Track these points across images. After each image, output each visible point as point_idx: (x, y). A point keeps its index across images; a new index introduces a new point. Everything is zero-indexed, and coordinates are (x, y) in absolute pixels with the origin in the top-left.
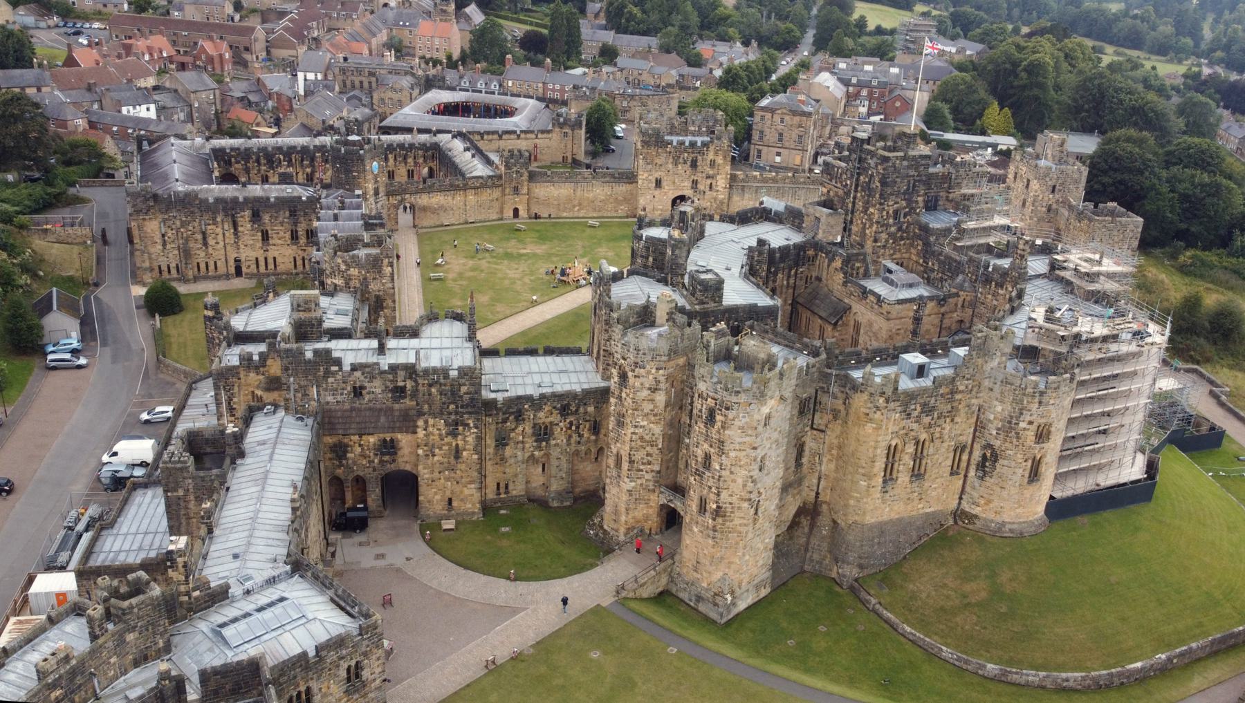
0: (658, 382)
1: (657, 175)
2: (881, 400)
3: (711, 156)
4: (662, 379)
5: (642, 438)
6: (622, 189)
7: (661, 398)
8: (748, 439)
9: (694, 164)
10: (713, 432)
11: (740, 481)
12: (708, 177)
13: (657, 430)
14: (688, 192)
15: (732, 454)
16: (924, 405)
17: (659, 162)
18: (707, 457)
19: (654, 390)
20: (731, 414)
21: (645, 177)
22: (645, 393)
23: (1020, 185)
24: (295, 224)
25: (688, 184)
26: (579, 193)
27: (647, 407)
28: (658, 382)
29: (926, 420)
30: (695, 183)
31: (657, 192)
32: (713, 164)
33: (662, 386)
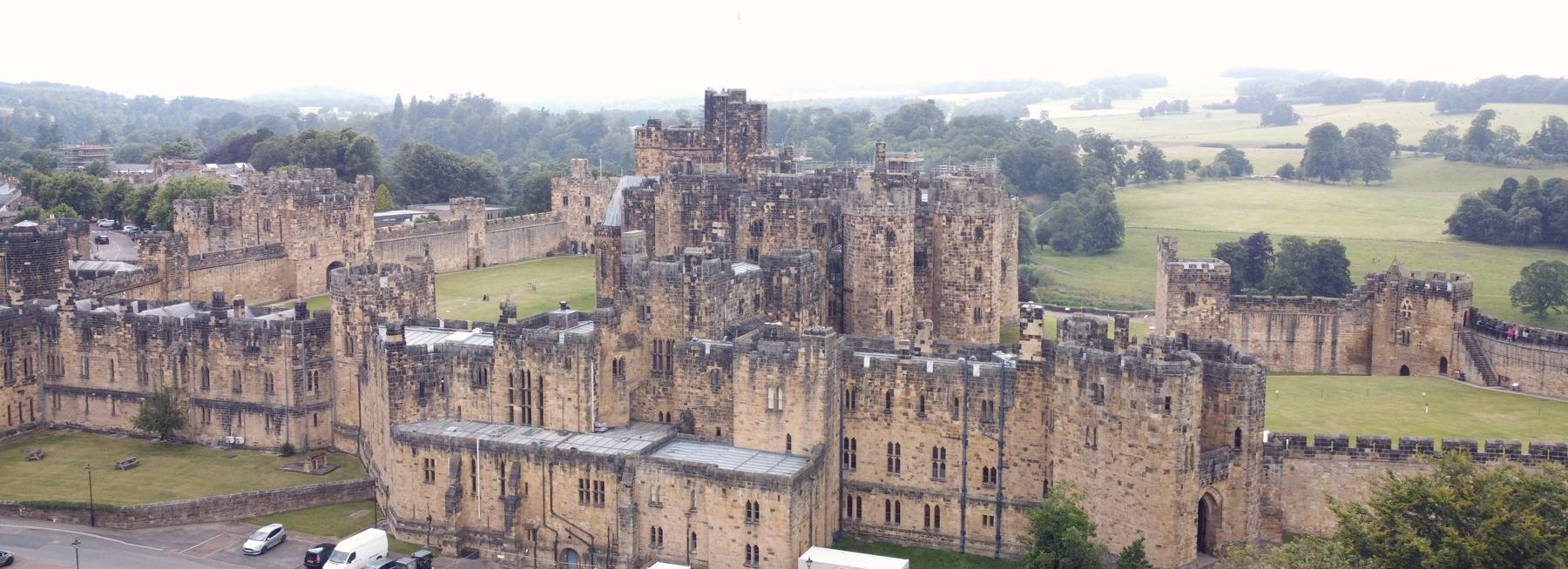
1: (312, 240)
3: (356, 211)
6: (274, 265)
9: (343, 226)
10: (983, 248)
12: (357, 236)
14: (340, 258)
17: (312, 224)
18: (979, 271)
21: (297, 249)
23: (576, 207)
24: (10, 353)
25: (339, 247)
26: (235, 277)
30: (345, 244)
31: (312, 262)
32: (359, 221)
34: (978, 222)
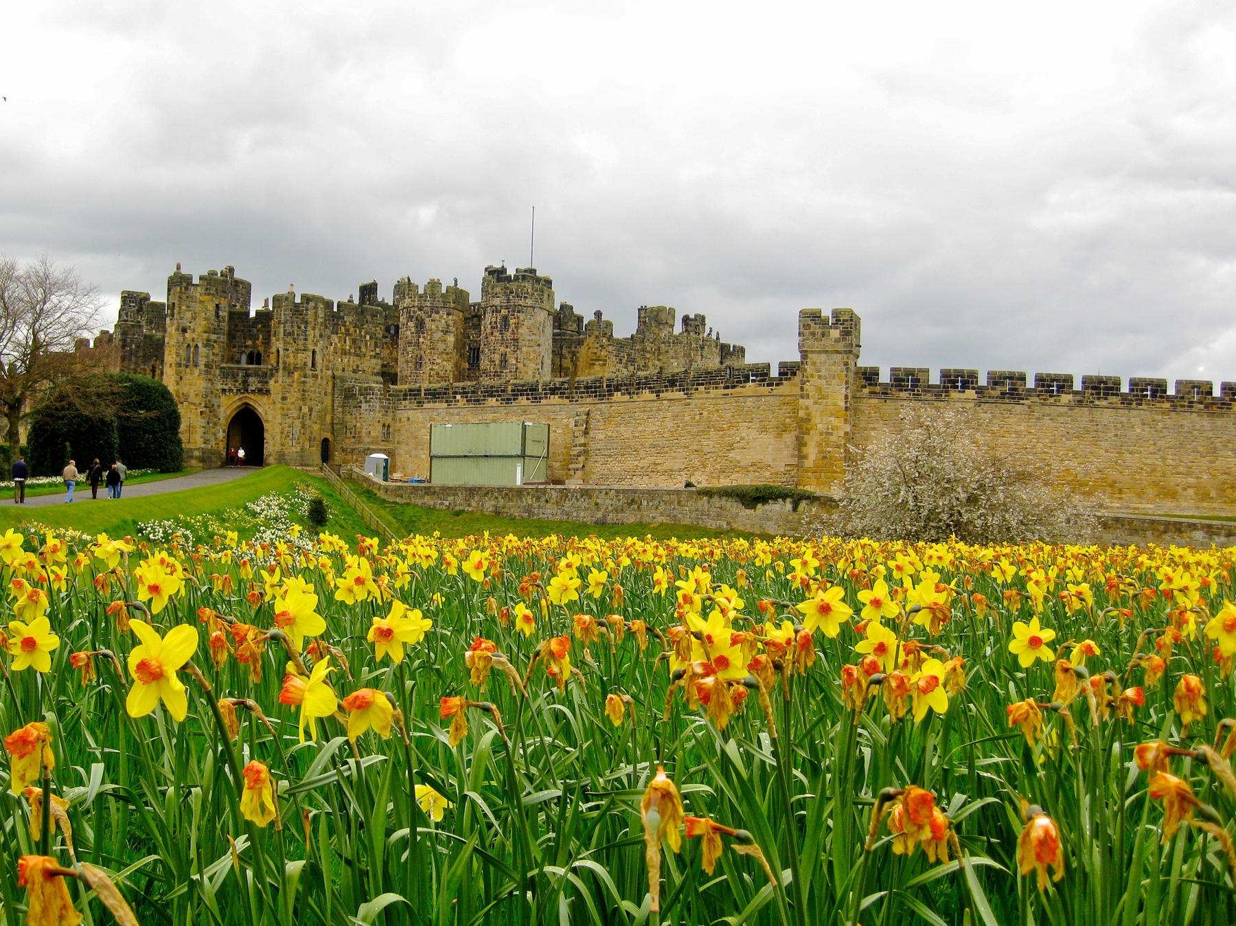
0: (448, 326)
2: (605, 340)
4: (451, 323)
5: (438, 374)
7: (451, 339)
8: (533, 337)
11: (530, 373)
13: (449, 366)
15: (524, 349)
16: (629, 355)
19: (446, 332)
20: (522, 316)
22: (438, 335)
27: (441, 346)
28: (448, 326)
29: (631, 368)
33: (453, 329)
34: (504, 312)
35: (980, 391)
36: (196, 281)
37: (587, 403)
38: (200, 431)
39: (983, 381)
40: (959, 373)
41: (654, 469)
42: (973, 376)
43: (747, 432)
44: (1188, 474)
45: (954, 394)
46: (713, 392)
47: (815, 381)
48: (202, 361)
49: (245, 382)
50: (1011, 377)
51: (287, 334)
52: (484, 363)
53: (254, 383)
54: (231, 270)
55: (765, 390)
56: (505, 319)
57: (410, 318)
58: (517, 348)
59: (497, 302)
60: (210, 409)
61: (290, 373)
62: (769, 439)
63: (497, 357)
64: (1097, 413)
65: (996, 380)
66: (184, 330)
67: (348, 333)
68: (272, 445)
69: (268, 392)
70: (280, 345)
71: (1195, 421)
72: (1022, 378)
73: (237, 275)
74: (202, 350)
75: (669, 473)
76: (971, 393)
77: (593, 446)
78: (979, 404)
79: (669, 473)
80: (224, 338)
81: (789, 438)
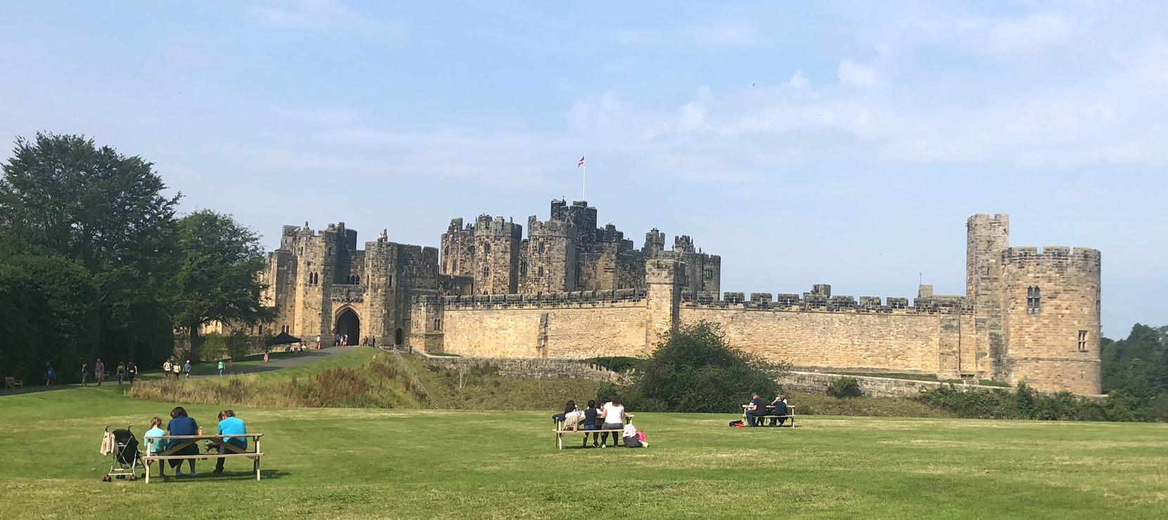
10: (544, 255)
35: (746, 304)
36: (316, 234)
37: (547, 309)
38: (319, 326)
39: (748, 298)
40: (734, 295)
41: (576, 349)
42: (742, 295)
43: (623, 327)
44: (867, 350)
45: (731, 306)
46: (607, 305)
47: (654, 300)
48: (320, 282)
49: (348, 295)
50: (763, 296)
51: (374, 266)
52: (529, 273)
53: (353, 295)
54: (342, 225)
55: (632, 304)
56: (542, 244)
57: (481, 243)
58: (550, 263)
59: (536, 233)
60: (326, 311)
61: (375, 290)
62: (634, 330)
63: (536, 269)
64: (814, 316)
65: (755, 298)
66: (309, 264)
67: (415, 264)
68: (364, 333)
69: (362, 301)
70: (370, 273)
71: (870, 318)
72: (770, 296)
73: (347, 227)
74: (320, 277)
75: (585, 350)
76: (740, 306)
77: (549, 334)
78: (745, 310)
79: (585, 350)
80: (334, 268)
81: (643, 330)
